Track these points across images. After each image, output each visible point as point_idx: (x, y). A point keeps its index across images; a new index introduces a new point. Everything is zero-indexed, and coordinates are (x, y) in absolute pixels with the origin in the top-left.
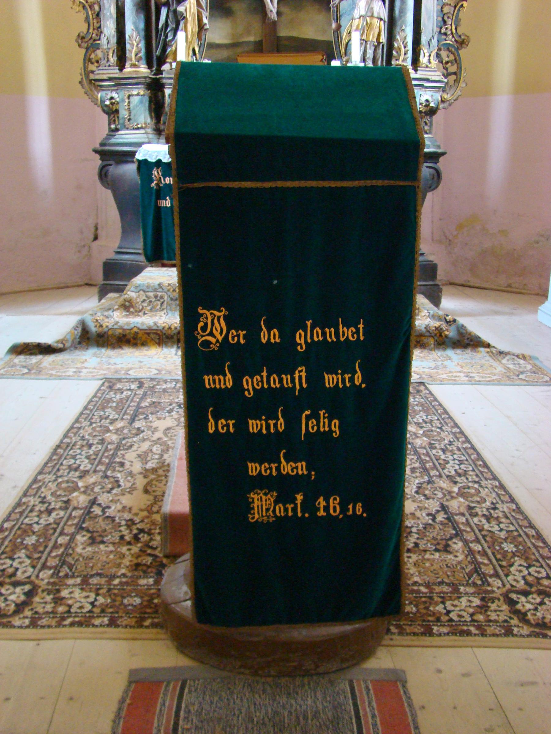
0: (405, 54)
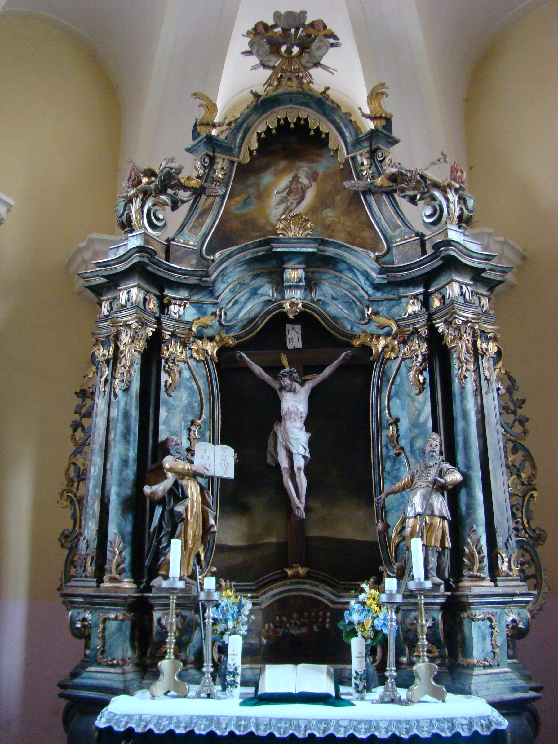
0: (480, 562)
